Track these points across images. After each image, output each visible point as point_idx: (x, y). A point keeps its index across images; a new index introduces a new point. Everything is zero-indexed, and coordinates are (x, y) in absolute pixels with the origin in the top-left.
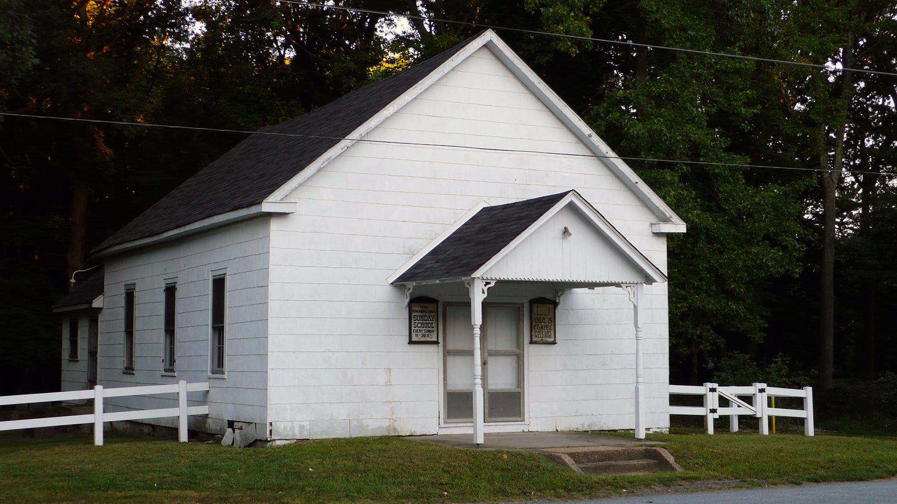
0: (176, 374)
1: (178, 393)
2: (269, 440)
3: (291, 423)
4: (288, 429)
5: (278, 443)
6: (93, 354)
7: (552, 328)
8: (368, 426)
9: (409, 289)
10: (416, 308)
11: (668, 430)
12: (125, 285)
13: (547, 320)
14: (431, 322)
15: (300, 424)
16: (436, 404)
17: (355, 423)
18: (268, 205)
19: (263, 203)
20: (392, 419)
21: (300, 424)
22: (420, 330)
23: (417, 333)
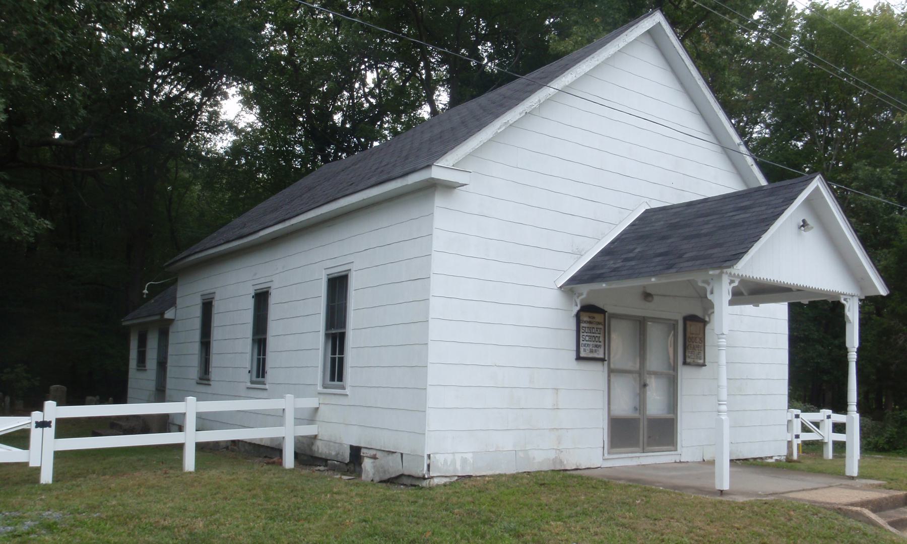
0: (267, 387)
1: (284, 409)
2: (426, 477)
4: (449, 464)
5: (436, 481)
6: (162, 365)
7: (702, 348)
8: (534, 458)
9: (582, 294)
10: (585, 317)
11: (785, 457)
12: (202, 295)
13: (698, 340)
14: (598, 335)
15: (462, 457)
16: (599, 432)
17: (521, 454)
18: (439, 172)
19: (433, 168)
20: (559, 449)
21: (462, 457)
22: (588, 345)
23: (585, 348)
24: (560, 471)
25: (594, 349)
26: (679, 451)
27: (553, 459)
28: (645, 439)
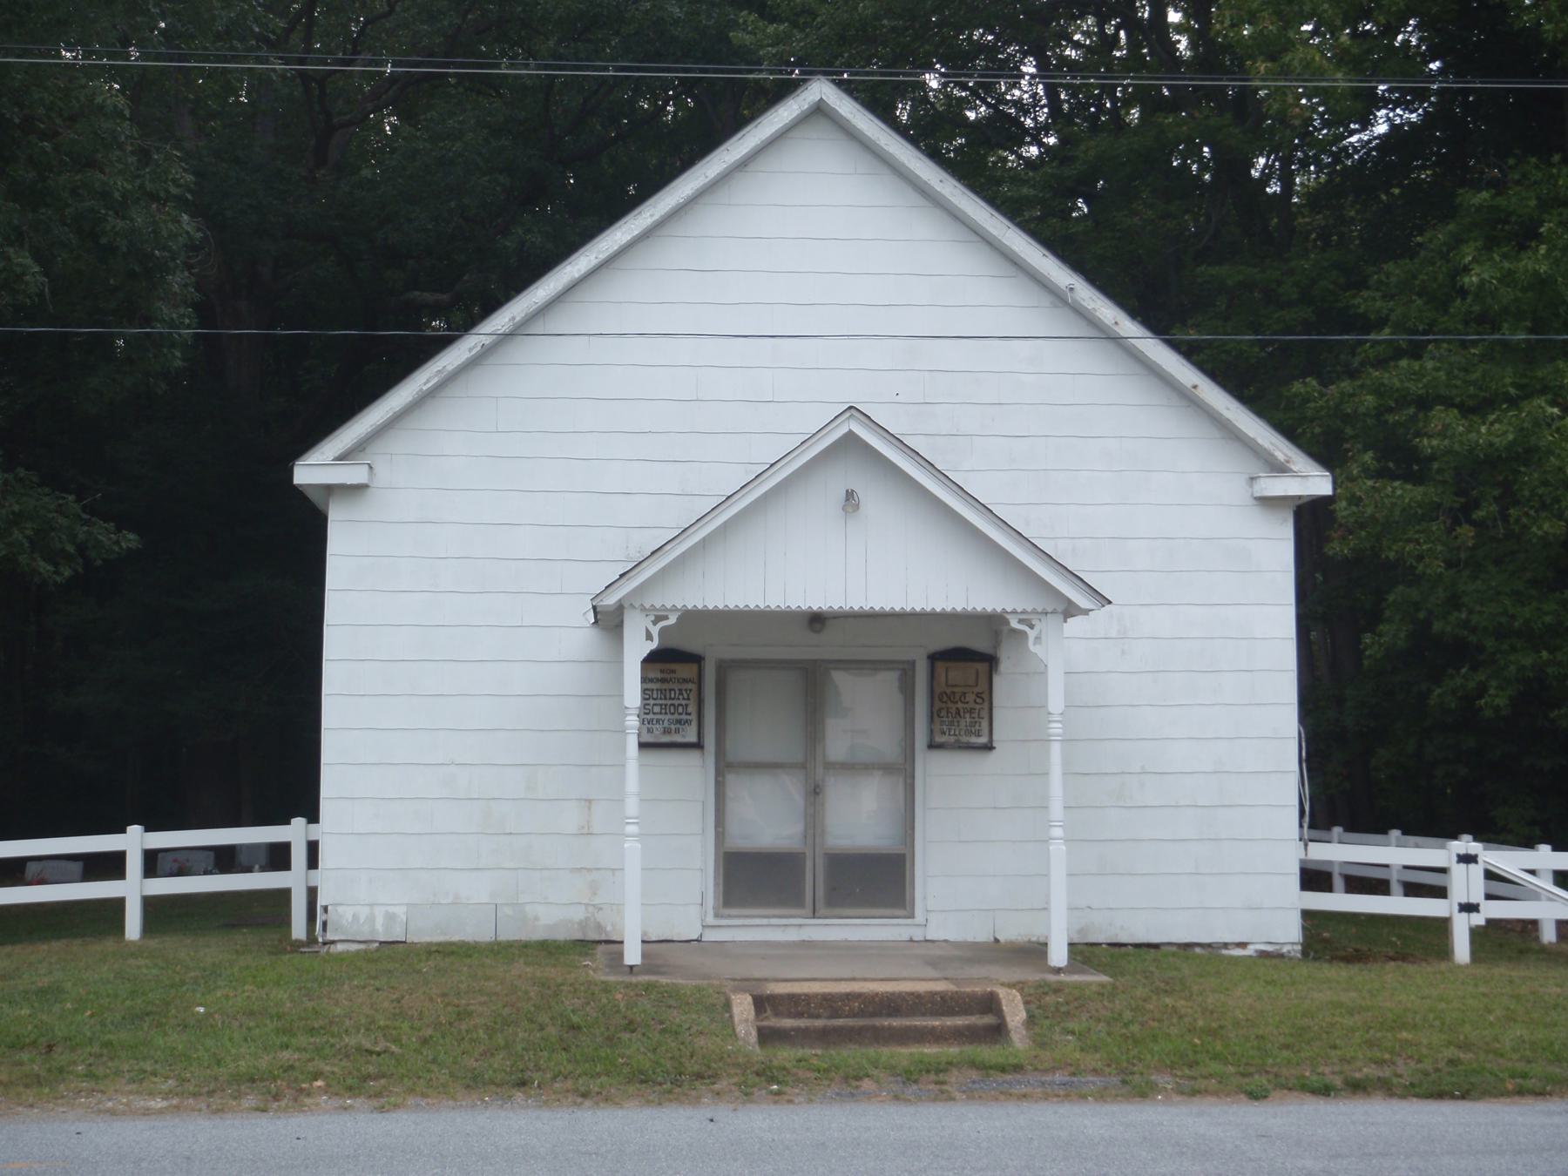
4: (362, 921)
5: (340, 947)
7: (985, 713)
8: (536, 918)
11: (1299, 947)
13: (970, 698)
14: (684, 702)
17: (508, 911)
20: (594, 905)
21: (387, 912)
22: (658, 721)
23: (650, 726)
24: (599, 942)
26: (919, 916)
27: (580, 923)
28: (820, 892)
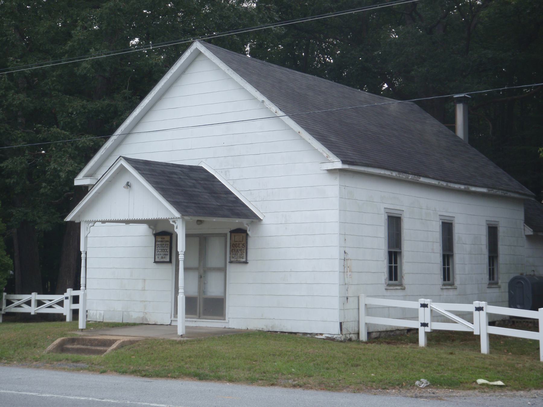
3: (96, 311)
5: (91, 322)
7: (245, 251)
8: (132, 316)
10: (159, 239)
13: (241, 245)
14: (166, 248)
15: (100, 312)
17: (125, 313)
20: (145, 312)
21: (100, 312)
25: (164, 256)
